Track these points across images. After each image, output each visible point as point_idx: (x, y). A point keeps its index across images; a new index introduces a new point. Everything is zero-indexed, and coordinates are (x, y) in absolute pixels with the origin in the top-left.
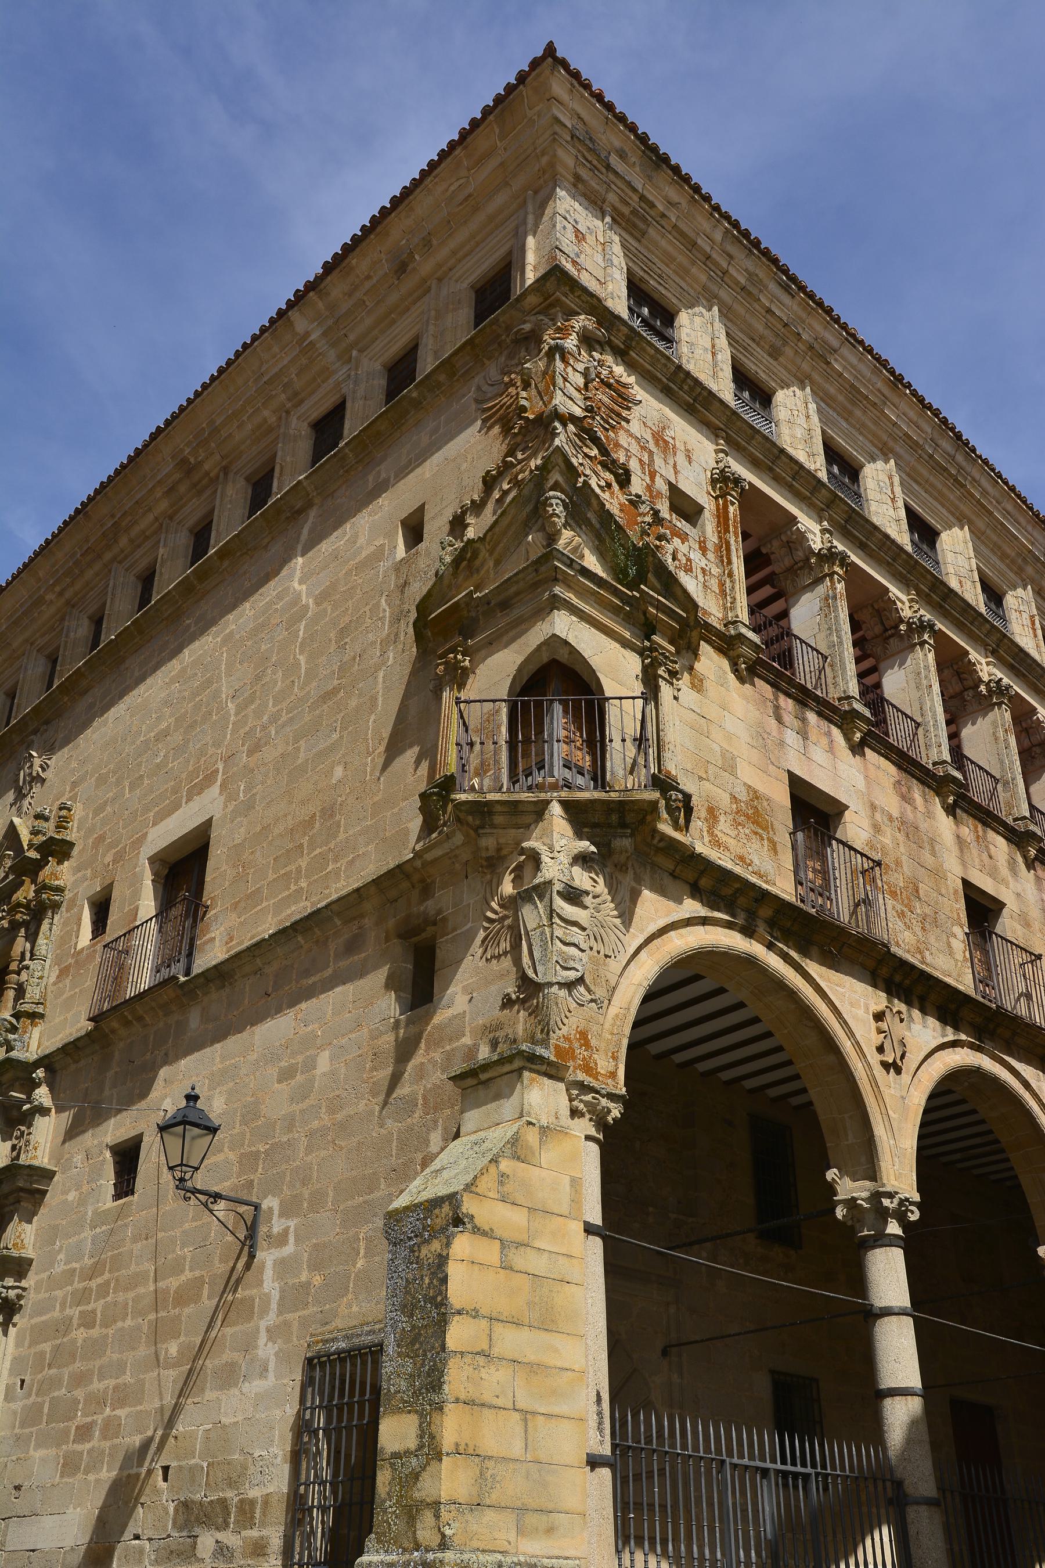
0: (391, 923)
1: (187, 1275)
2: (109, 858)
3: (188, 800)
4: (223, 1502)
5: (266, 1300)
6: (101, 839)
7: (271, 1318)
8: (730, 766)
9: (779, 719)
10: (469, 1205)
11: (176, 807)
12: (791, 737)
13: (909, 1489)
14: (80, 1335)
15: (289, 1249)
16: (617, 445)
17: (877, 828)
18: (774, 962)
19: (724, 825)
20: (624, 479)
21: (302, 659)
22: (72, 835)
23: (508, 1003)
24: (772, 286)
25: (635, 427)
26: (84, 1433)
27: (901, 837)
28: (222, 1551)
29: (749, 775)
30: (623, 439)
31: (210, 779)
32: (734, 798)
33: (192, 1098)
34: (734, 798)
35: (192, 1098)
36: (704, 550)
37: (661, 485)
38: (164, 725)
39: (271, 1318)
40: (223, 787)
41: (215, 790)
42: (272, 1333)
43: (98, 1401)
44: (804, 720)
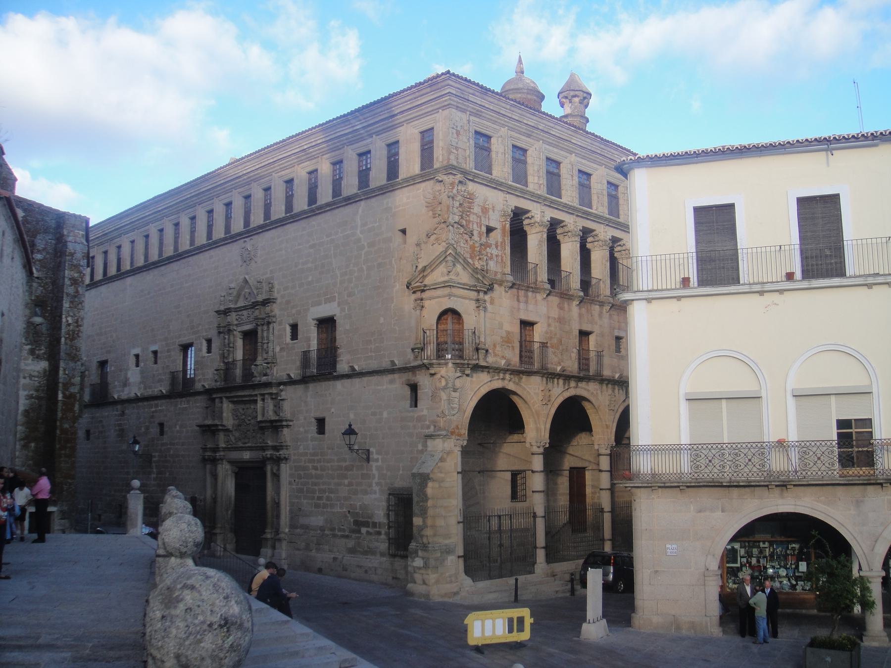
0: (404, 379)
1: (347, 463)
2: (294, 311)
3: (325, 303)
4: (368, 522)
5: (374, 475)
6: (288, 302)
7: (376, 480)
8: (501, 326)
9: (518, 301)
10: (431, 476)
11: (320, 304)
12: (522, 305)
13: (537, 514)
14: (313, 472)
15: (380, 463)
16: (469, 221)
17: (549, 325)
18: (511, 386)
19: (498, 348)
20: (472, 234)
21: (365, 267)
22: (276, 295)
23: (438, 416)
24: (528, 115)
25: (476, 209)
26: (320, 498)
27: (557, 324)
28: (368, 532)
29: (507, 327)
30: (473, 218)
31: (332, 299)
32: (502, 337)
33: (350, 425)
34: (502, 337)
35: (350, 425)
36: (497, 247)
37: (484, 229)
38: (310, 265)
39: (376, 480)
40: (339, 304)
41: (335, 304)
42: (377, 484)
43: (324, 491)
44: (527, 297)
